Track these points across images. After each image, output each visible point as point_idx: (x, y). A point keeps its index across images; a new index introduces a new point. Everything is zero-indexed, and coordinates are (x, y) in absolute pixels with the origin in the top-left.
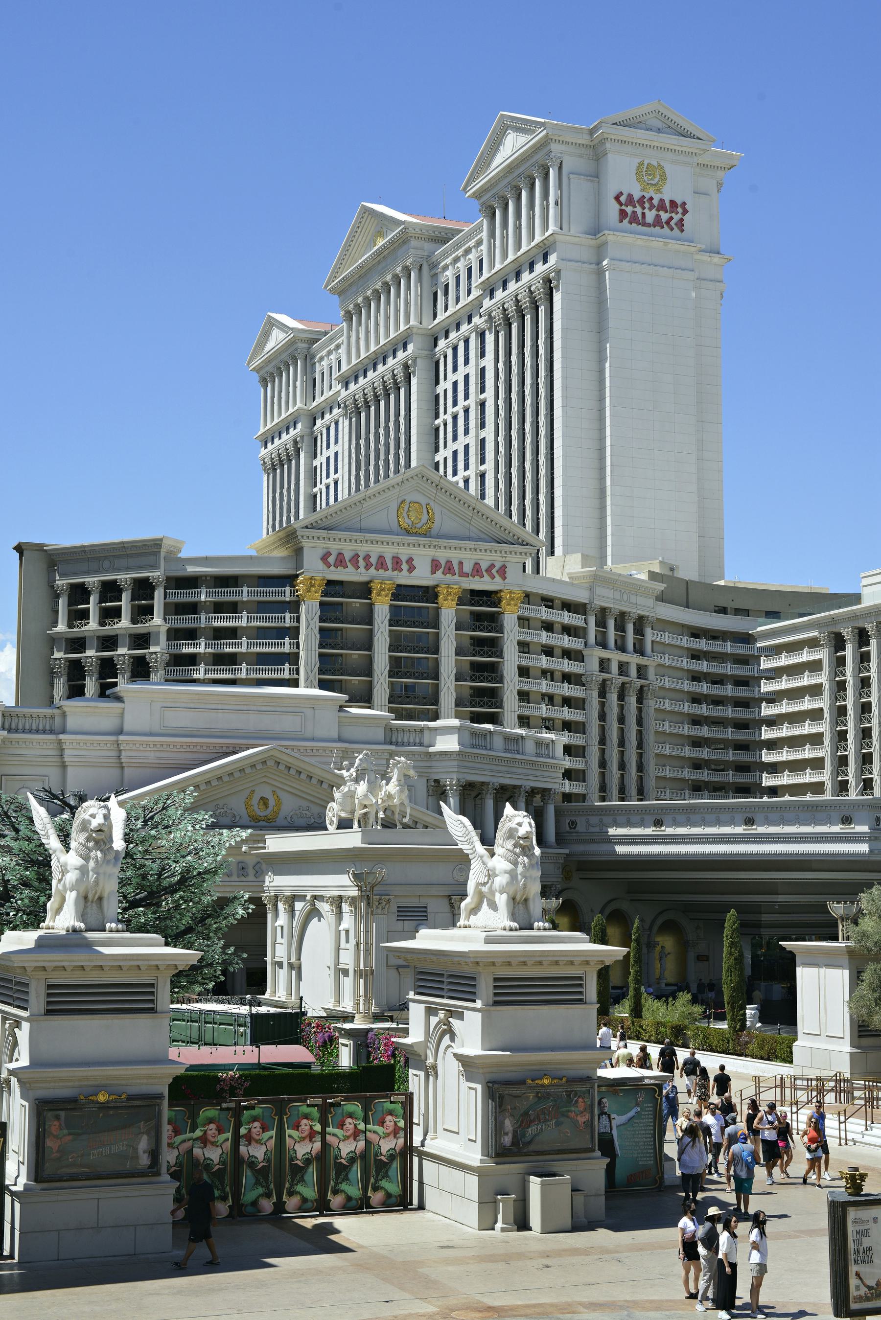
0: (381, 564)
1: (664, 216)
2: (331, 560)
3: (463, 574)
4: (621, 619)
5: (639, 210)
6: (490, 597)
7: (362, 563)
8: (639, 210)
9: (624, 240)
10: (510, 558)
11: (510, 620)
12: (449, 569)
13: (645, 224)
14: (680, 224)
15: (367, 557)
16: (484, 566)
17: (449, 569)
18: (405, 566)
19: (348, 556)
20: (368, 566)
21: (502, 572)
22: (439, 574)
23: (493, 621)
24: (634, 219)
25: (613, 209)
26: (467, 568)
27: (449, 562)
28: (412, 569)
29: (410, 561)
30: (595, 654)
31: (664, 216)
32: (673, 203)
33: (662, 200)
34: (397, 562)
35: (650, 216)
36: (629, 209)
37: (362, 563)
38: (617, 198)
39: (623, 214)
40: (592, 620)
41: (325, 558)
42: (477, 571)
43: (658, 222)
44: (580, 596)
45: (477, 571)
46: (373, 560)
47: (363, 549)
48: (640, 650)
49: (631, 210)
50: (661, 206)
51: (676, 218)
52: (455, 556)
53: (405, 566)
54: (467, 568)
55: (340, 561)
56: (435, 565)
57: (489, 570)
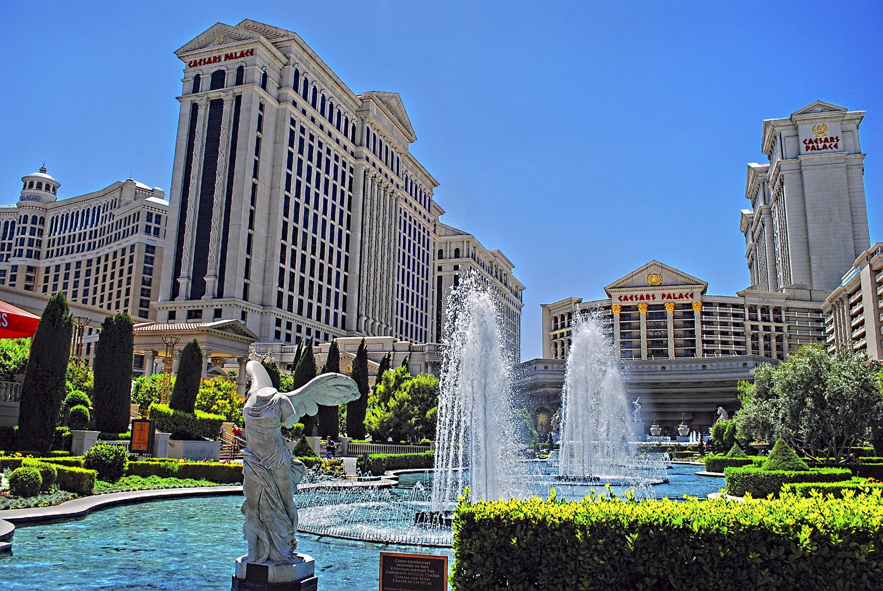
0: (642, 298)
3: (675, 298)
4: (765, 310)
6: (690, 306)
10: (694, 290)
12: (669, 297)
15: (636, 296)
17: (669, 297)
21: (692, 296)
26: (677, 296)
28: (654, 298)
29: (653, 296)
30: (748, 324)
40: (747, 310)
41: (620, 299)
42: (681, 296)
44: (741, 301)
45: (681, 296)
47: (635, 293)
48: (777, 320)
52: (671, 292)
54: (677, 296)
55: (626, 298)
56: (664, 296)
57: (686, 296)
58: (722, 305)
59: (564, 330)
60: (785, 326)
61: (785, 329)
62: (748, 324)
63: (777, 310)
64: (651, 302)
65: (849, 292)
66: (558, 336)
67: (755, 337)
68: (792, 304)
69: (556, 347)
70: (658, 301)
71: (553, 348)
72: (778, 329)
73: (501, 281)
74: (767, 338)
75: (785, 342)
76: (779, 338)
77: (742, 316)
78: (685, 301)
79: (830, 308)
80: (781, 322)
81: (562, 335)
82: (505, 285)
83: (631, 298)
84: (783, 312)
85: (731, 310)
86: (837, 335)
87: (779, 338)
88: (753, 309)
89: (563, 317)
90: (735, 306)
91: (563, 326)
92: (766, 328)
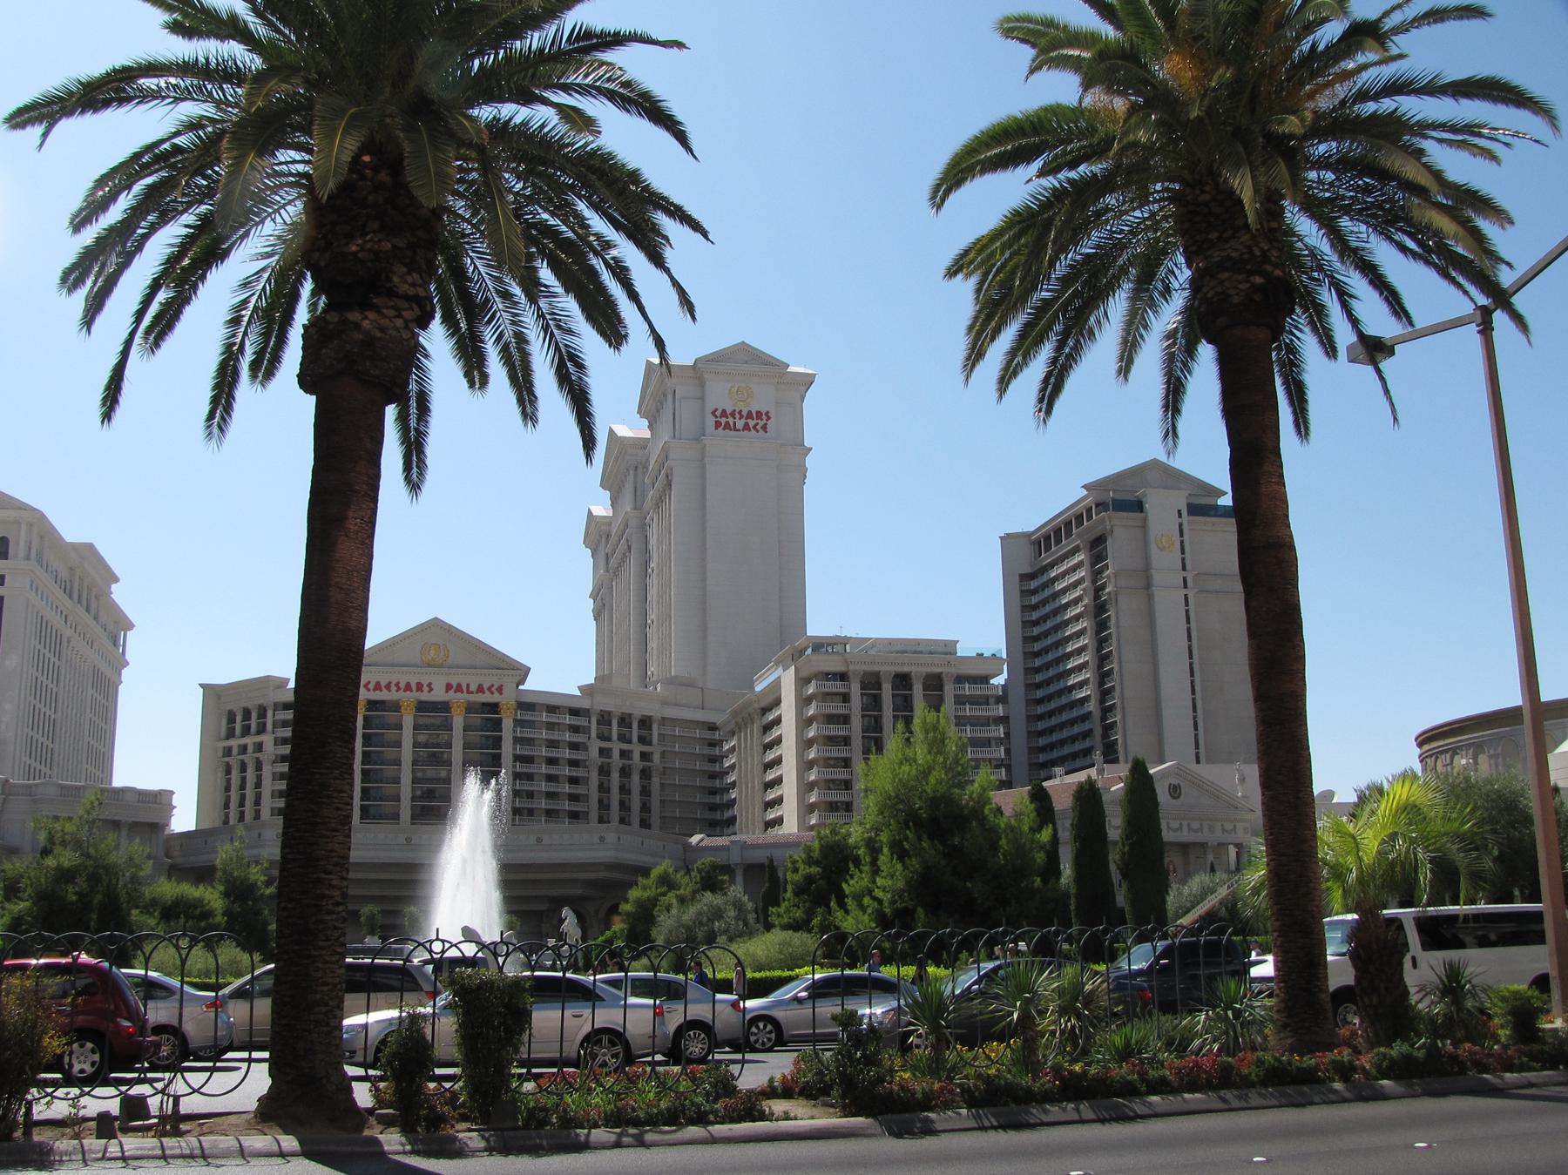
1: (751, 423)
2: (371, 686)
3: (469, 692)
4: (625, 721)
5: (731, 420)
6: (494, 707)
7: (394, 688)
8: (731, 420)
9: (721, 444)
11: (507, 724)
12: (459, 689)
13: (736, 430)
14: (764, 428)
15: (397, 685)
16: (486, 686)
17: (459, 689)
18: (426, 689)
19: (383, 683)
20: (398, 689)
21: (500, 690)
22: (451, 693)
23: (497, 725)
24: (727, 426)
25: (711, 421)
26: (473, 688)
27: (459, 685)
28: (431, 690)
29: (429, 685)
31: (751, 423)
32: (759, 415)
33: (750, 413)
34: (420, 687)
35: (740, 424)
36: (723, 420)
37: (394, 688)
38: (713, 413)
39: (718, 425)
40: (594, 720)
42: (480, 689)
43: (746, 427)
44: (585, 704)
45: (480, 689)
46: (402, 685)
47: (394, 679)
49: (724, 420)
50: (750, 415)
51: (761, 423)
53: (426, 689)
54: (473, 688)
56: (449, 687)
58: (552, 709)
59: (249, 741)
60: (656, 750)
61: (656, 758)
62: (595, 746)
63: (645, 723)
64: (425, 696)
65: (763, 704)
66: (235, 751)
67: (604, 771)
68: (670, 713)
69: (228, 772)
70: (439, 694)
71: (221, 774)
72: (645, 756)
73: (88, 610)
74: (625, 772)
75: (656, 780)
76: (645, 774)
77: (586, 730)
78: (487, 698)
79: (732, 726)
80: (650, 744)
81: (244, 749)
82: (96, 618)
83: (388, 687)
84: (655, 727)
85: (568, 719)
86: (739, 776)
87: (645, 774)
88: (605, 718)
89: (247, 714)
90: (574, 712)
91: (246, 731)
92: (624, 754)
